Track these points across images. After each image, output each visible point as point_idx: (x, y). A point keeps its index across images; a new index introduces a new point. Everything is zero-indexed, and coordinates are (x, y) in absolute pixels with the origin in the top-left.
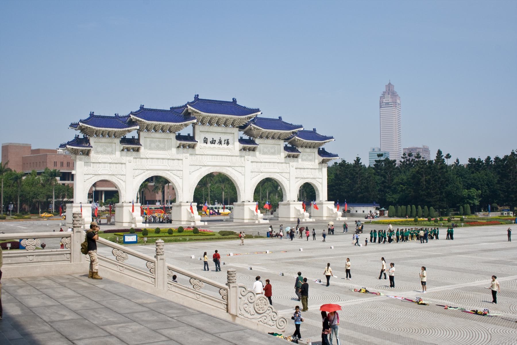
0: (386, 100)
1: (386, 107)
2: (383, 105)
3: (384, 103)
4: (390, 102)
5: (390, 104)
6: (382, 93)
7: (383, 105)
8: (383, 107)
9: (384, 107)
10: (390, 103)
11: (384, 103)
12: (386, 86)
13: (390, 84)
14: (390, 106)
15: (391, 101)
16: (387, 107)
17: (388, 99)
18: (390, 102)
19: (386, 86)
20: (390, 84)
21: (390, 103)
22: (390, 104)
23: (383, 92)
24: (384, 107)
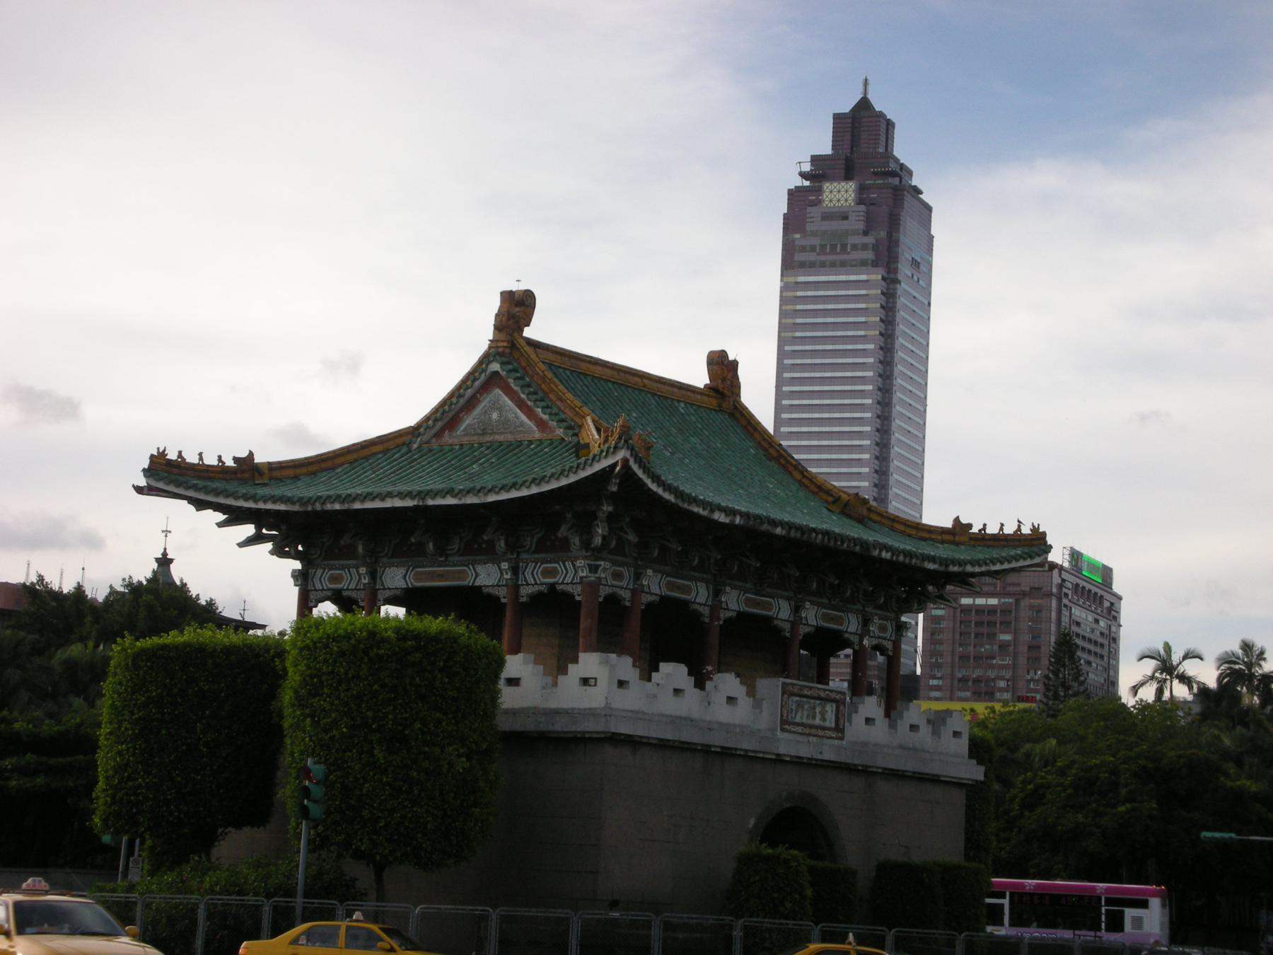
2: (803, 249)
3: (814, 234)
4: (855, 233)
5: (855, 247)
6: (807, 167)
10: (853, 240)
11: (814, 234)
12: (838, 118)
13: (864, 104)
18: (855, 233)
19: (838, 118)
20: (864, 104)
22: (855, 247)
23: (815, 159)
24: (812, 265)
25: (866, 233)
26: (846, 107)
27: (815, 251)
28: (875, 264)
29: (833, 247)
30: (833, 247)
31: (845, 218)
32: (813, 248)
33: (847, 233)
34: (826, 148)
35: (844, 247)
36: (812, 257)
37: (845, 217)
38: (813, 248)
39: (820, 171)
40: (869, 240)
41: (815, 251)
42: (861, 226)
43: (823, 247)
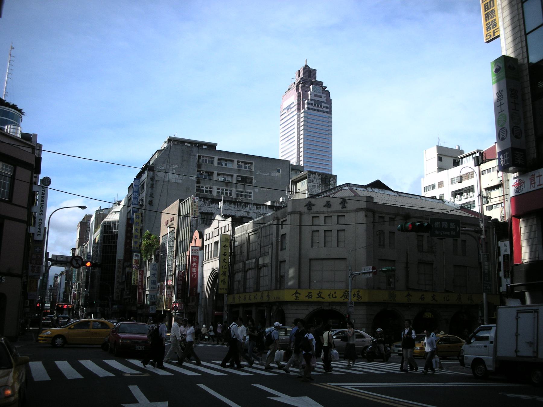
1: (315, 110)
4: (324, 102)
5: (324, 107)
9: (312, 109)
13: (306, 65)
15: (325, 101)
16: (318, 111)
17: (321, 94)
20: (306, 65)
21: (324, 105)
22: (324, 107)
25: (326, 103)
26: (304, 65)
27: (313, 105)
29: (318, 106)
30: (318, 106)
32: (312, 104)
35: (321, 106)
38: (312, 104)
41: (313, 105)
42: (325, 101)
43: (315, 105)
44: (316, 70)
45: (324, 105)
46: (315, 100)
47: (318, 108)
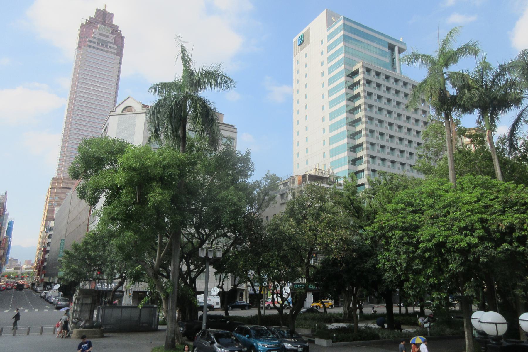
0: (100, 34)
2: (90, 41)
4: (111, 43)
7: (90, 41)
8: (90, 46)
9: (94, 47)
11: (95, 38)
14: (110, 50)
17: (108, 34)
18: (111, 43)
21: (109, 45)
22: (110, 47)
23: (91, 18)
24: (94, 47)
25: (115, 44)
28: (117, 54)
29: (102, 45)
30: (102, 45)
31: (108, 37)
32: (94, 43)
33: (108, 42)
34: (93, 16)
35: (106, 46)
36: (94, 45)
37: (108, 37)
38: (94, 43)
39: (91, 24)
40: (116, 47)
43: (98, 44)
44: (112, 15)
45: (109, 45)
46: (99, 39)
47: (102, 48)
